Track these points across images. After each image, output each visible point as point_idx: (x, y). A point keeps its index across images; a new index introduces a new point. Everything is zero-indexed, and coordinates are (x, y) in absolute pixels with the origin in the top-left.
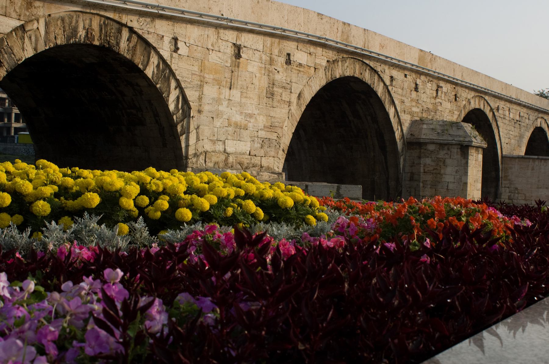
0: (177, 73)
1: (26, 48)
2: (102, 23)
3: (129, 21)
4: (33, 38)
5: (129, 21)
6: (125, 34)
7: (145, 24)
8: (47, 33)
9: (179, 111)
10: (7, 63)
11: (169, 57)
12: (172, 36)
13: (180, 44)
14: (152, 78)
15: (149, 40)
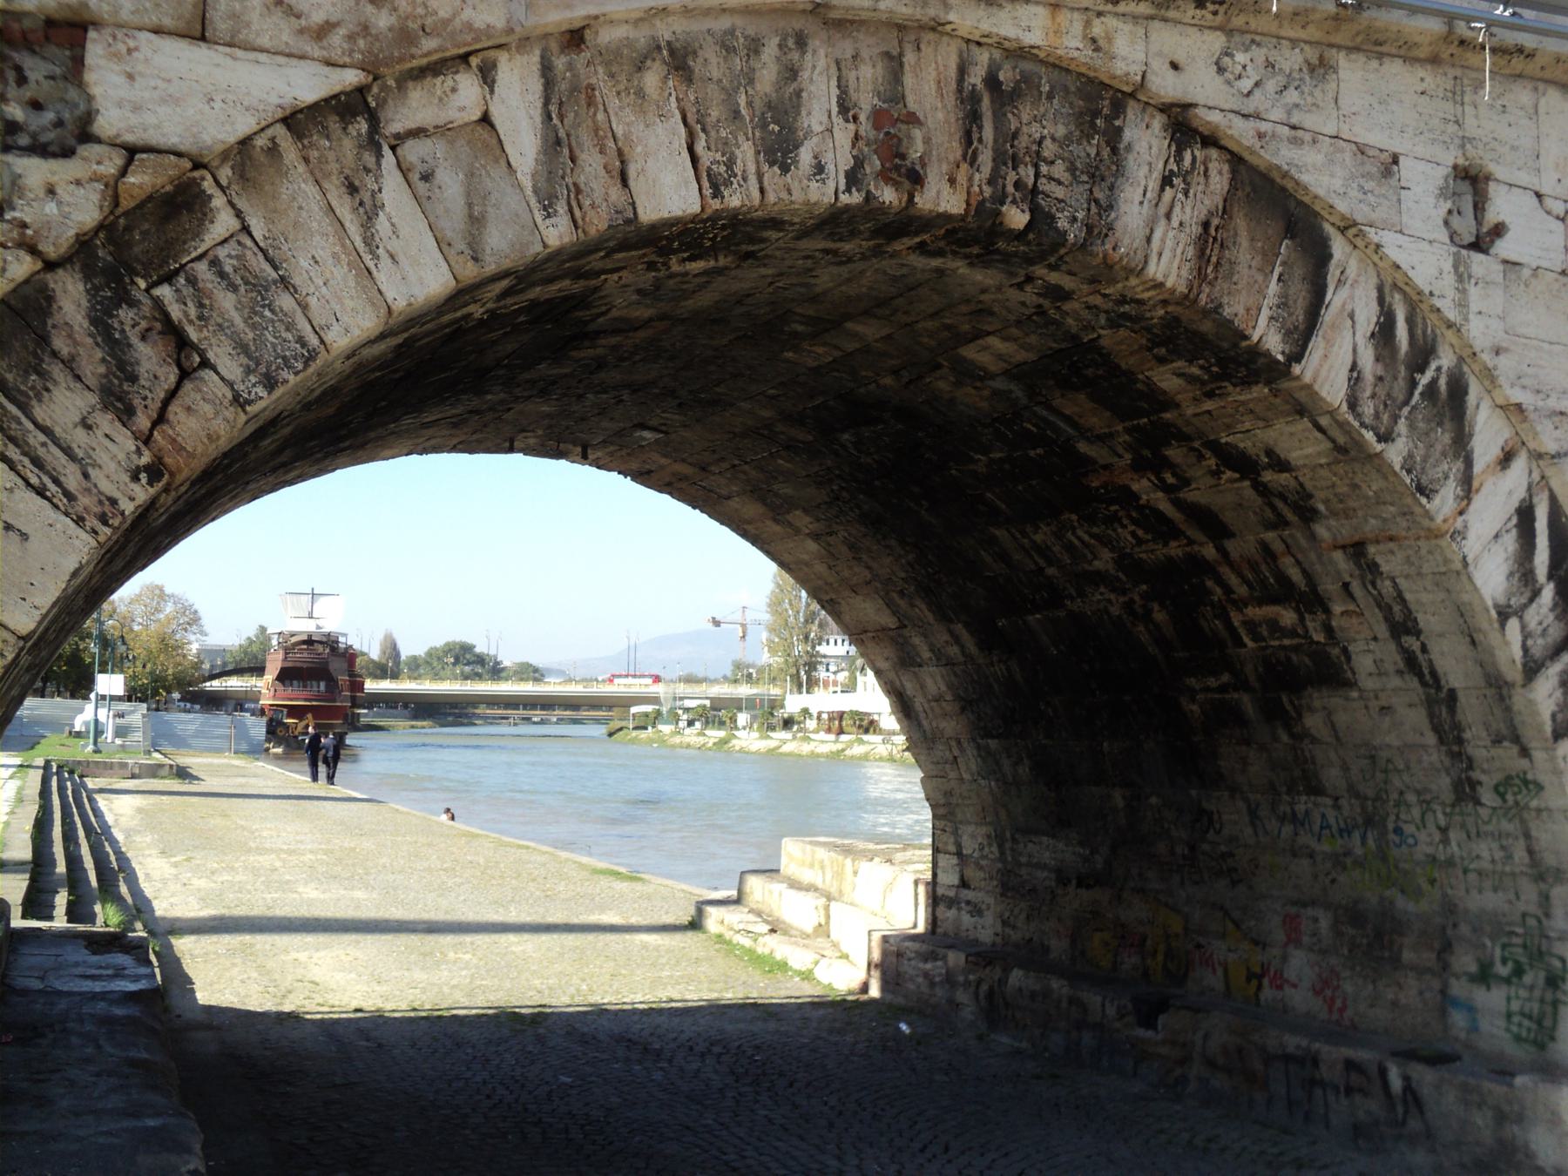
0: (1505, 366)
1: (394, 245)
2: (976, 78)
3: (1159, 68)
4: (450, 183)
5: (1159, 68)
6: (1146, 143)
7: (1271, 86)
8: (555, 145)
9: (1536, 593)
10: (242, 348)
11: (1449, 279)
12: (1450, 157)
13: (1502, 205)
14: (1353, 404)
15: (1305, 178)
